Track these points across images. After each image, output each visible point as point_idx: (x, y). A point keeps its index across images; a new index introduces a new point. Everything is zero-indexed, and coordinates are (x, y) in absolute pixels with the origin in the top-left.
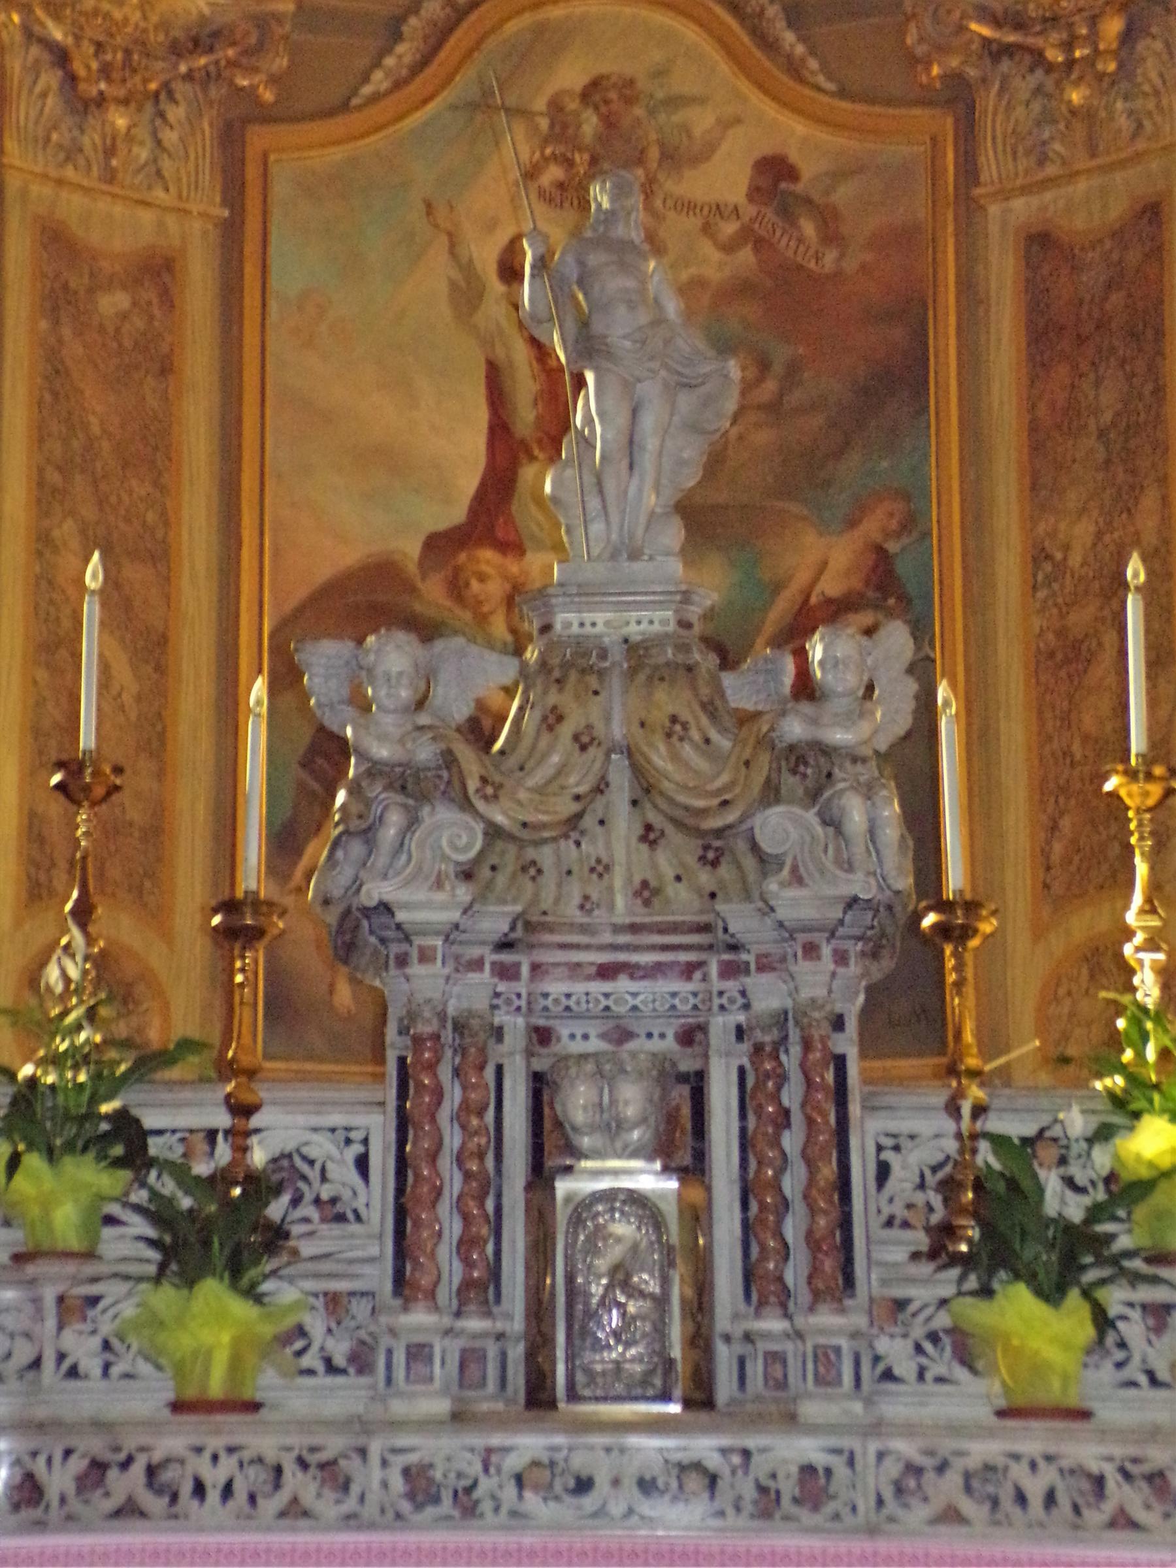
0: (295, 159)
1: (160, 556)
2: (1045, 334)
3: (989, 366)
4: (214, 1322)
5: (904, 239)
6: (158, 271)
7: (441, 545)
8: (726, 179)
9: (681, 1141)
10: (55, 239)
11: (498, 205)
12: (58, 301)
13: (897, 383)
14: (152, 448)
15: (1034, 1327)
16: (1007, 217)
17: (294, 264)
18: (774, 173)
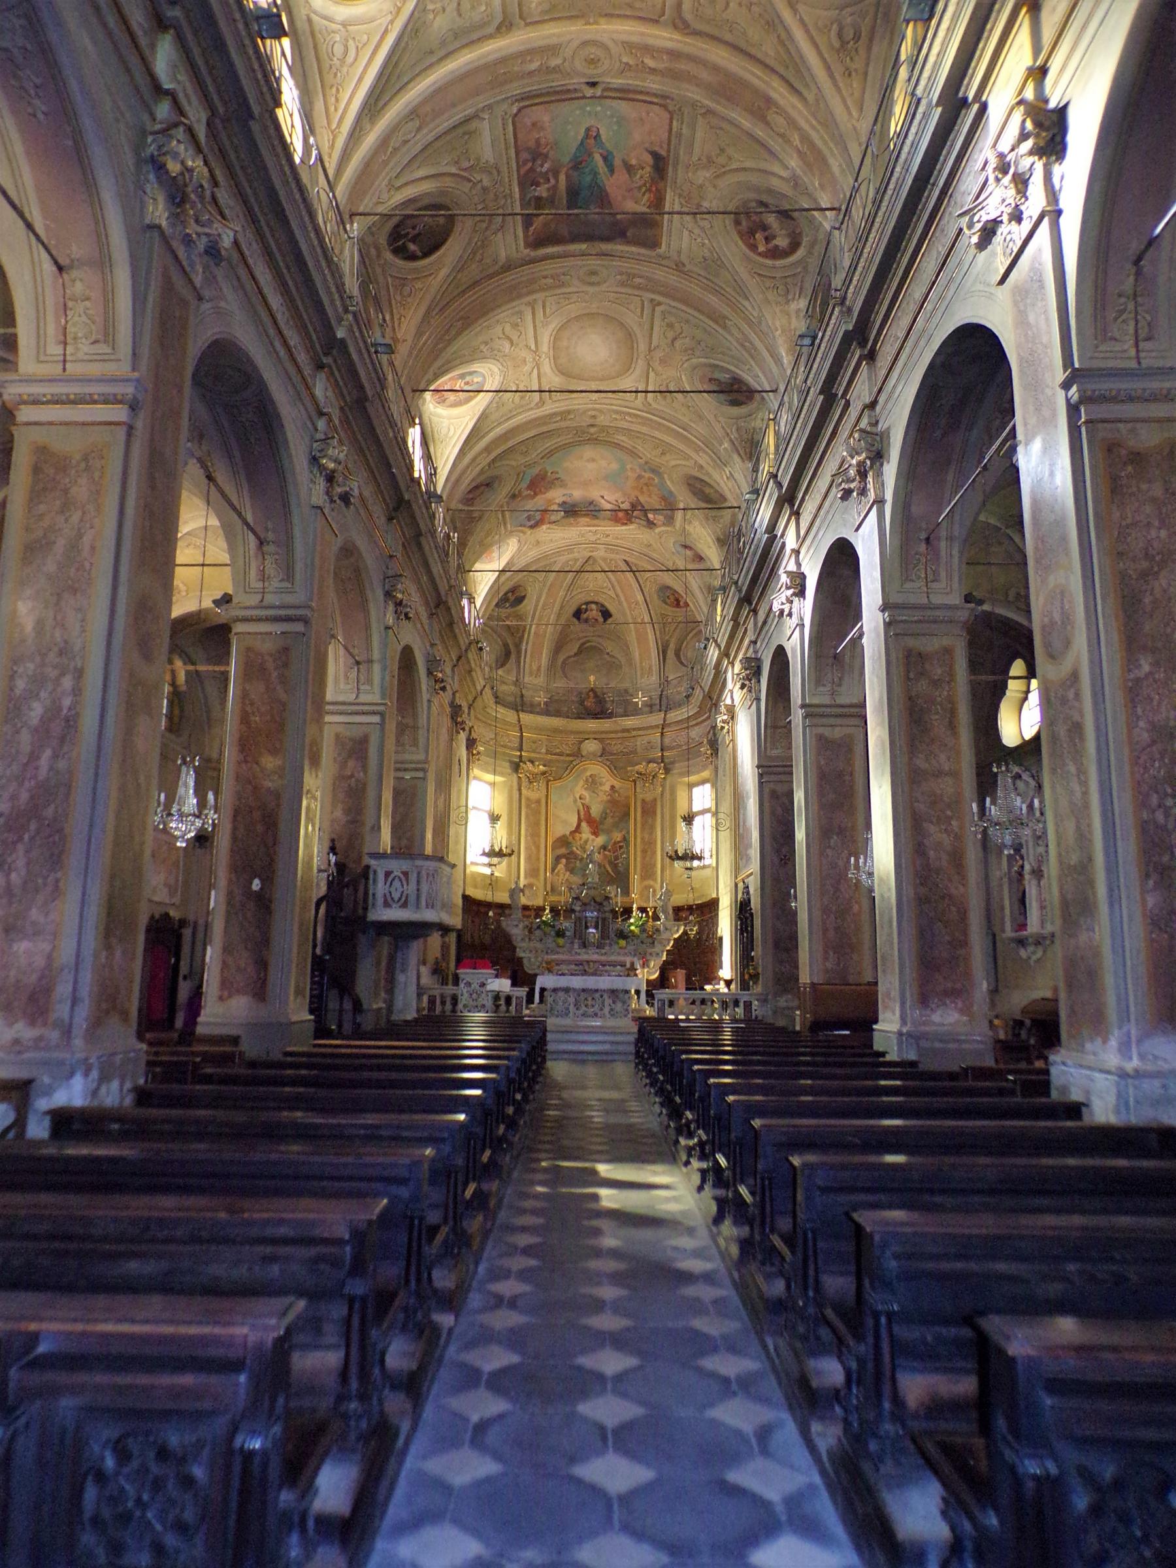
0: (554, 785)
1: (539, 836)
2: (644, 812)
3: (636, 814)
4: (561, 941)
5: (627, 797)
6: (538, 802)
7: (572, 833)
8: (607, 788)
9: (596, 927)
10: (528, 799)
11: (580, 790)
12: (528, 806)
13: (627, 814)
14: (537, 824)
15: (623, 943)
16: (640, 796)
17: (553, 797)
18: (613, 787)
